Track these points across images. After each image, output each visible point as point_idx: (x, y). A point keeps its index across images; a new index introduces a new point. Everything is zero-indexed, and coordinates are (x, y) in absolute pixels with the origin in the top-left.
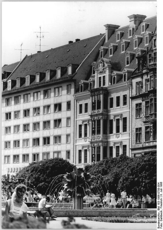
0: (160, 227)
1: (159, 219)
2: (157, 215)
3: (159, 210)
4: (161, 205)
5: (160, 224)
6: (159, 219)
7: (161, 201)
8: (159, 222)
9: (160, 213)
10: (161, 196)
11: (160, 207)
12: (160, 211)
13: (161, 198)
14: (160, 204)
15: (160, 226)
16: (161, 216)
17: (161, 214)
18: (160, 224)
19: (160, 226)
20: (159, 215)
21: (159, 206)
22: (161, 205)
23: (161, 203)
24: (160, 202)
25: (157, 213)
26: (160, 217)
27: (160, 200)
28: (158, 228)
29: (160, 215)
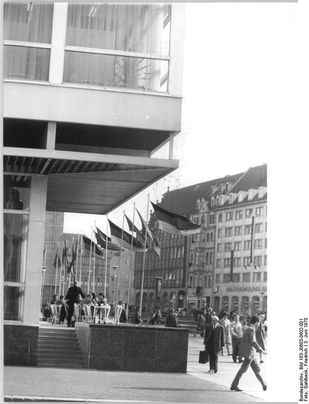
0: (303, 399)
1: (302, 384)
4: (306, 360)
5: (304, 394)
6: (302, 384)
7: (306, 353)
8: (302, 390)
10: (306, 344)
11: (304, 363)
12: (303, 370)
13: (306, 347)
14: (304, 358)
15: (304, 397)
16: (306, 379)
17: (306, 376)
18: (304, 394)
19: (304, 397)
20: (302, 377)
21: (301, 361)
22: (306, 360)
23: (306, 356)
24: (304, 355)
26: (304, 381)
27: (304, 352)
28: (301, 400)
29: (304, 377)
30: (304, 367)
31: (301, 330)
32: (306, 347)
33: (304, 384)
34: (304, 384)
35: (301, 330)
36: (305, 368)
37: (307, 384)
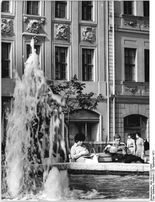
1: (151, 192)
2: (150, 189)
3: (151, 184)
4: (154, 180)
5: (152, 197)
6: (151, 192)
8: (151, 195)
9: (152, 188)
10: (153, 172)
11: (152, 181)
12: (152, 185)
13: (154, 174)
14: (153, 179)
15: (152, 198)
16: (153, 190)
17: (154, 188)
18: (152, 197)
19: (152, 198)
20: (152, 188)
21: (151, 181)
22: (154, 180)
23: (154, 178)
24: (153, 178)
25: (150, 187)
26: (153, 191)
27: (152, 176)
28: (151, 200)
29: (153, 189)
30: (152, 183)
31: (151, 164)
32: (154, 174)
33: (152, 192)
34: (152, 192)
35: (151, 170)
36: (153, 184)
37: (154, 192)
